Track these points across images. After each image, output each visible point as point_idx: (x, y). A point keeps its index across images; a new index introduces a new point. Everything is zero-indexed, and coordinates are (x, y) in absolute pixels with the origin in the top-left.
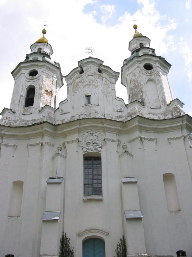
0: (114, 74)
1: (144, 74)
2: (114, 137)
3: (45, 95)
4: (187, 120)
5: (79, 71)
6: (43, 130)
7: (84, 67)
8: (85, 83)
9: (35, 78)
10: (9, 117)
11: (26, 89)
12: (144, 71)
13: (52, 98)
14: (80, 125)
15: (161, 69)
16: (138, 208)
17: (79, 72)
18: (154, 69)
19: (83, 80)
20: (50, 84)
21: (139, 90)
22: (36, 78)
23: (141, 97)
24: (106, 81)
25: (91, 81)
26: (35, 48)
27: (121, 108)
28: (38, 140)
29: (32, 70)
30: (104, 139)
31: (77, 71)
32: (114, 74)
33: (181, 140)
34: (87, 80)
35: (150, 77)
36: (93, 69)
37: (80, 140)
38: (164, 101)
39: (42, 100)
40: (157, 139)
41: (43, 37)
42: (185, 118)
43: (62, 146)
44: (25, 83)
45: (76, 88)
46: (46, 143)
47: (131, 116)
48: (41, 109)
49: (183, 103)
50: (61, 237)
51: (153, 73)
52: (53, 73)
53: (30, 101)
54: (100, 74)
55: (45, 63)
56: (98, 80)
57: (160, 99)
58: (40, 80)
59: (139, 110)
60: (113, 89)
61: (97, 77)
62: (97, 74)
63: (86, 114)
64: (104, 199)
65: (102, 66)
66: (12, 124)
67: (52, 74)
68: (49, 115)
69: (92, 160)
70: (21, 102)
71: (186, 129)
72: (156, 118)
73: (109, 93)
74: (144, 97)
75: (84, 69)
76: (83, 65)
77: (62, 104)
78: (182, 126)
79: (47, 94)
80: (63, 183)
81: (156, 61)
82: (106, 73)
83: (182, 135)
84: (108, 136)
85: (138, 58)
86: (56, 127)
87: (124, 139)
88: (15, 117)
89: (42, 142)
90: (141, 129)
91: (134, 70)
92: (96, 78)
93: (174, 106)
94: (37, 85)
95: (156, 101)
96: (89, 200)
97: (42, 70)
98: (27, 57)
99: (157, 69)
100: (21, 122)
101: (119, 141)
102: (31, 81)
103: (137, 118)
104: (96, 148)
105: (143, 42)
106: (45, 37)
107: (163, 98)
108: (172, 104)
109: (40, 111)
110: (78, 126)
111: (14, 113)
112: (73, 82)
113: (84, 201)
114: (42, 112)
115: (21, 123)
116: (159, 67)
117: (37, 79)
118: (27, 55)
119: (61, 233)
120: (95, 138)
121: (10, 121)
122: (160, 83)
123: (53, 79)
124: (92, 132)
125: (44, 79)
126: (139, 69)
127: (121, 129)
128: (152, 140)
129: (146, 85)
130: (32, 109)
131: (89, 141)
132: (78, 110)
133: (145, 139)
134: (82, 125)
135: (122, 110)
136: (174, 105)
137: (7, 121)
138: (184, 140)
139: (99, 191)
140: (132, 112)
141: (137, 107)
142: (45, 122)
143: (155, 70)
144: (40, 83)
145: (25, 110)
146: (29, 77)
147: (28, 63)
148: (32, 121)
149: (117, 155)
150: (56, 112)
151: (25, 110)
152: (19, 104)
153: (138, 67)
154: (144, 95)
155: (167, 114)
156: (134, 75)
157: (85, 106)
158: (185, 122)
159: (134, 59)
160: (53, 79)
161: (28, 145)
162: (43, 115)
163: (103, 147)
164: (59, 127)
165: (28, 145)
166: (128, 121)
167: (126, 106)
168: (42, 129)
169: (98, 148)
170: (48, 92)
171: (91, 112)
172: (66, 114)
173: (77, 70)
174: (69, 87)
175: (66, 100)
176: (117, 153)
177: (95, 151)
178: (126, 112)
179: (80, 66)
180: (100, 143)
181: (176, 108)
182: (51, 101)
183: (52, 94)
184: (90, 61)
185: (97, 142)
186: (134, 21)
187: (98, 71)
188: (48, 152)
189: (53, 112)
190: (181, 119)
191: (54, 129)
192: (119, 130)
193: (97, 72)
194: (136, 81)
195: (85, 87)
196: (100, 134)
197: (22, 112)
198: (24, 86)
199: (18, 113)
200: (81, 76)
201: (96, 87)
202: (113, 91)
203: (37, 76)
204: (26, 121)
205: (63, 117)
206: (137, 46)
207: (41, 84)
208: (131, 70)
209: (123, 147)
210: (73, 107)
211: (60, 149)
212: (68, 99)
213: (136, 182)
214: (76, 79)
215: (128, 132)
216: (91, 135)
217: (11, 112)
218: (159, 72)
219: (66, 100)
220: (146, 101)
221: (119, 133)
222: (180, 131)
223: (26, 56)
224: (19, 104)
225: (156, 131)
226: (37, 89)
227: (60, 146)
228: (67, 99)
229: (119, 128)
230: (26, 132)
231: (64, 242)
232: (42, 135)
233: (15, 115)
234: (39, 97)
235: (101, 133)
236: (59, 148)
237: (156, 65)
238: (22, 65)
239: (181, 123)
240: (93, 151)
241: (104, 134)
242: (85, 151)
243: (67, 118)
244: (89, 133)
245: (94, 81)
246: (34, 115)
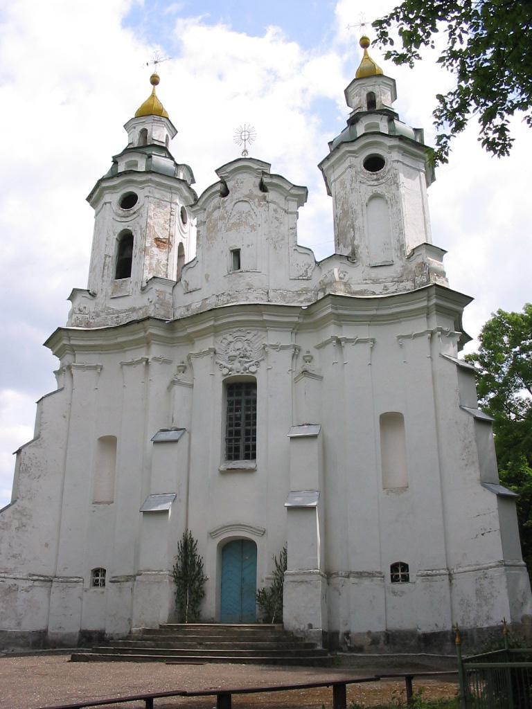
0: (294, 191)
1: (363, 183)
2: (285, 338)
3: (155, 250)
4: (439, 296)
5: (218, 191)
6: (147, 333)
7: (229, 181)
8: (231, 221)
9: (132, 212)
10: (85, 308)
11: (115, 240)
12: (363, 176)
13: (170, 254)
14: (215, 321)
15: (404, 164)
16: (316, 485)
17: (219, 194)
18: (387, 167)
19: (226, 213)
20: (165, 222)
21: (349, 222)
22: (135, 213)
23: (351, 241)
24: (275, 211)
25: (244, 215)
26: (133, 130)
27: (306, 272)
28: (140, 354)
29: (125, 194)
30: (263, 346)
31: (214, 193)
32: (294, 191)
33: (424, 340)
34: (234, 213)
35: (375, 189)
36: (248, 183)
37: (218, 351)
38: (402, 246)
39: (147, 262)
40: (373, 340)
41: (153, 96)
42: (433, 291)
43: (186, 364)
44: (113, 226)
45: (213, 234)
46: (155, 359)
47: (324, 290)
48: (144, 284)
49: (443, 250)
50: (179, 538)
51: (383, 178)
52: (172, 193)
53: (124, 268)
54: (263, 193)
55: (149, 177)
56: (260, 211)
57: (394, 244)
58: (142, 216)
59: (342, 276)
60: (291, 226)
61: (257, 204)
62: (256, 196)
63: (231, 293)
64: (258, 468)
65: (266, 176)
66: (91, 321)
67: (169, 195)
68: (161, 297)
69: (241, 394)
70: (106, 271)
71: (437, 314)
72: (378, 291)
73: (280, 238)
74: (356, 243)
75: (230, 185)
76: (227, 177)
77: (187, 270)
78: (428, 307)
79: (158, 246)
80: (183, 442)
81: (391, 147)
82: (276, 191)
83: (428, 327)
84: (274, 338)
85: (350, 144)
86: (173, 325)
87: (307, 342)
88: (97, 304)
89: (147, 357)
90: (341, 320)
91: (342, 174)
92: (253, 206)
93: (419, 260)
94: (138, 229)
95: (386, 246)
96: (229, 471)
97: (146, 192)
98: (115, 160)
99: (392, 167)
100: (108, 314)
101: (297, 349)
102: (124, 219)
103: (329, 300)
104: (245, 367)
105: (376, 90)
106: (157, 94)
107: (398, 241)
108: (416, 254)
109: (143, 289)
110: (212, 323)
111: (94, 295)
112: (207, 218)
113: (222, 473)
114: (146, 290)
115: (109, 317)
116: (398, 161)
117: (135, 216)
118: (113, 157)
119: (183, 531)
120: (246, 346)
121: (88, 316)
122: (397, 202)
123: (171, 208)
124: (239, 334)
125: (151, 214)
126: (352, 172)
127: (301, 321)
128: (365, 341)
129: (365, 212)
130: (131, 283)
131: (234, 353)
132: (213, 287)
133: (347, 340)
134: (219, 319)
135: (309, 274)
136: (421, 257)
137: (80, 316)
138: (431, 339)
139: (251, 454)
140: (326, 281)
141: (336, 271)
142: (149, 318)
143: (389, 171)
144: (142, 222)
145: (116, 286)
146: (121, 211)
147: (115, 178)
148: (129, 310)
149: (289, 377)
150: (177, 288)
151: (116, 288)
152: (103, 276)
153: (350, 167)
154: (357, 236)
155: (404, 278)
156: (343, 184)
157: (229, 274)
158: (434, 301)
159: (341, 147)
160: (171, 208)
161: (122, 364)
162: (149, 299)
163: (261, 363)
164: (177, 324)
165: (122, 364)
166: (318, 301)
167: (318, 264)
168: (146, 332)
169: (250, 366)
170: (161, 241)
171: (240, 288)
172: (194, 293)
173: (214, 190)
174: (201, 228)
175: (194, 259)
176: (290, 372)
177: (245, 374)
178: (317, 277)
179: (223, 182)
180: (255, 356)
181: (423, 265)
182: (167, 260)
183: (170, 243)
185: (248, 354)
186: (363, 25)
187: (258, 188)
188: (160, 377)
189: (169, 290)
190: (425, 294)
192: (297, 323)
194: (346, 201)
195: (229, 230)
196: (256, 337)
197: (110, 294)
198: (111, 233)
199: (102, 296)
200: (224, 202)
201: (253, 228)
202: (292, 231)
203: (136, 207)
204: (118, 312)
206: (360, 101)
207: (144, 226)
208: (339, 171)
209: (304, 359)
210: (207, 277)
211: (183, 369)
212: (198, 259)
213: (315, 437)
214: (213, 211)
215: (318, 325)
216: (237, 339)
217: (89, 296)
218: (396, 175)
219: (195, 262)
220: (362, 252)
221: (296, 329)
222: (425, 319)
223: (112, 160)
224: (103, 276)
225: (373, 320)
226: (137, 239)
227: (183, 363)
228: (196, 258)
229: (296, 319)
230: (116, 338)
231: (187, 547)
232: (147, 342)
233: (97, 301)
234: (140, 258)
235: (260, 333)
236: (180, 368)
238: (104, 185)
239: (425, 304)
240: (239, 374)
241: (264, 335)
242: (225, 373)
243: (196, 303)
244: (236, 335)
245: (249, 214)
246: (132, 301)
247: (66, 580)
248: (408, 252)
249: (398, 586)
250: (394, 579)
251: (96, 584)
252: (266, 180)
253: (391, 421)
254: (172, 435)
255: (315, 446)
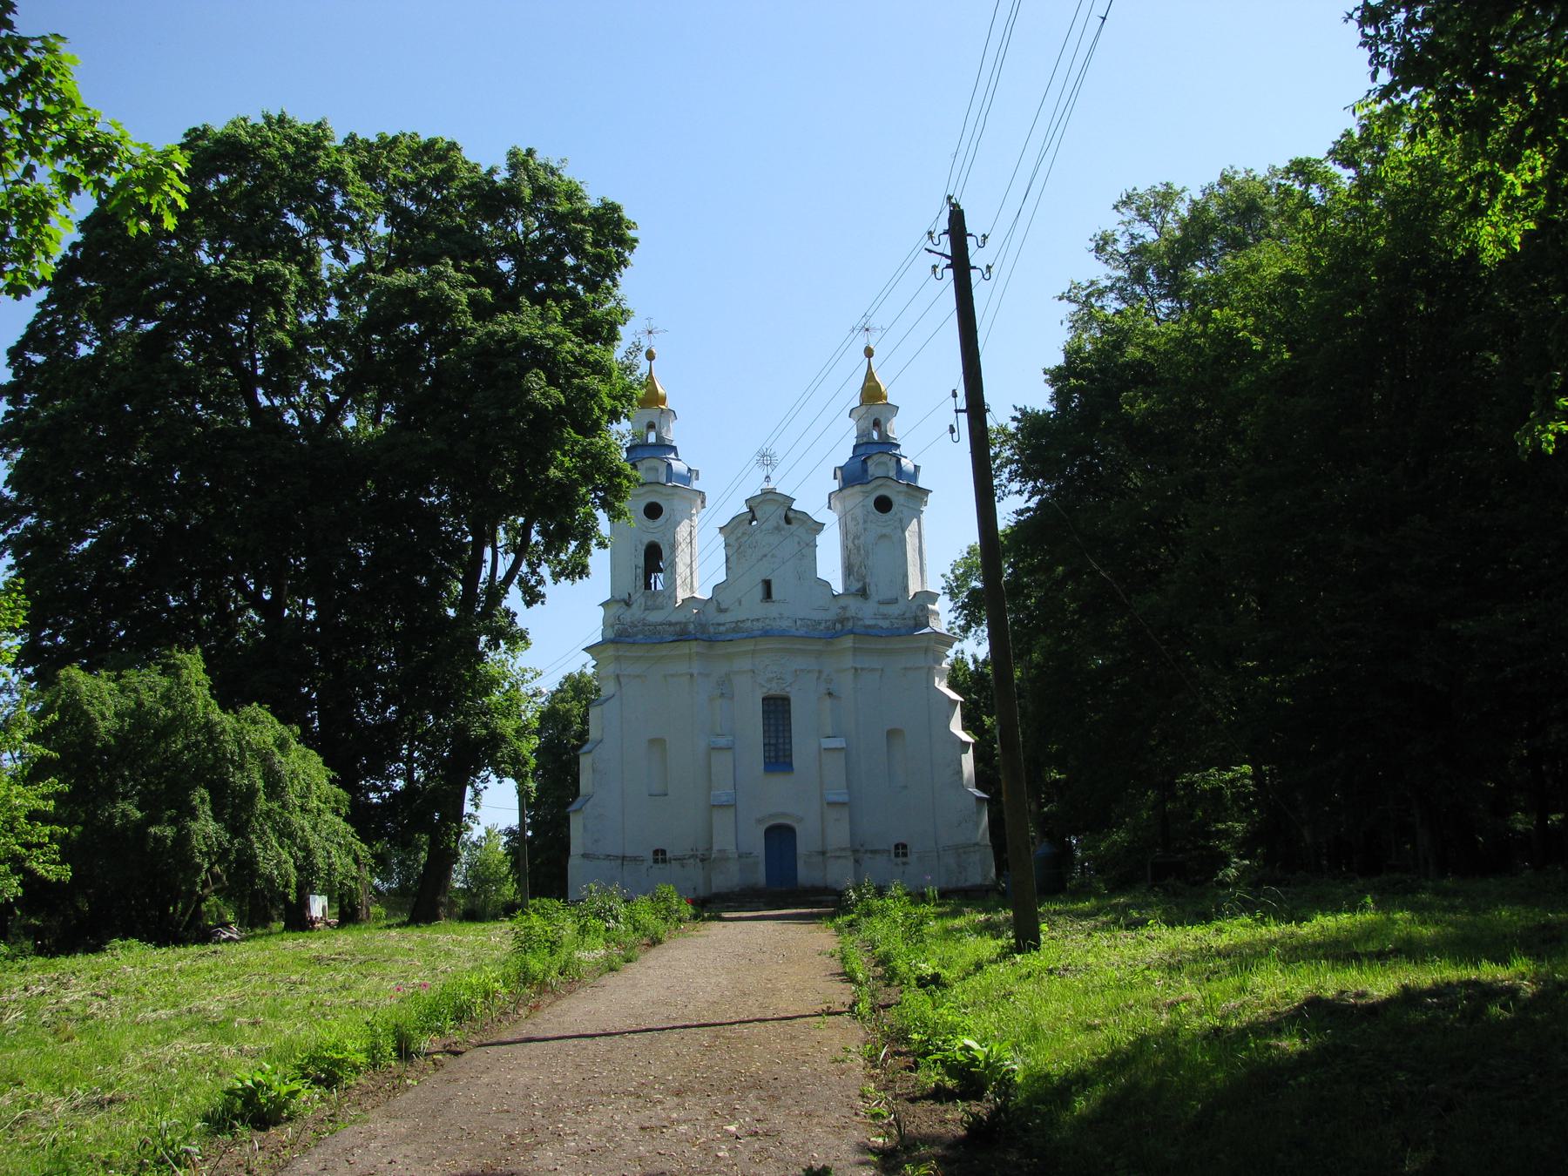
36: (774, 514)
69: (777, 709)
101: (820, 672)
141: (854, 605)
179: (751, 510)
184: (769, 495)
191: (701, 632)
193: (782, 522)
205: (722, 618)
220: (872, 590)
237: (898, 500)
247: (635, 859)
248: (912, 594)
249: (900, 860)
250: (897, 855)
251: (656, 861)
252: (791, 515)
253: (892, 734)
254: (722, 742)
255: (843, 754)
